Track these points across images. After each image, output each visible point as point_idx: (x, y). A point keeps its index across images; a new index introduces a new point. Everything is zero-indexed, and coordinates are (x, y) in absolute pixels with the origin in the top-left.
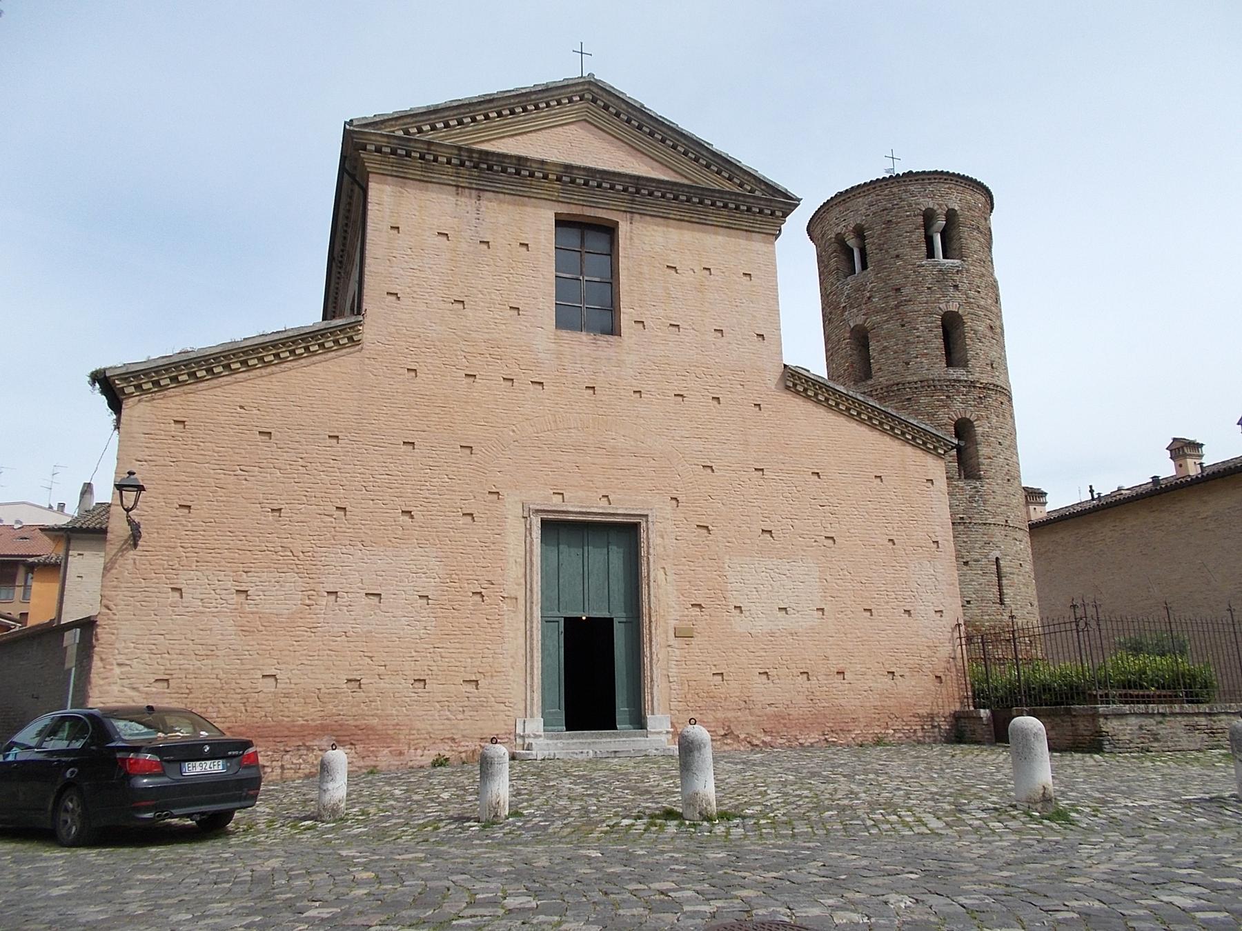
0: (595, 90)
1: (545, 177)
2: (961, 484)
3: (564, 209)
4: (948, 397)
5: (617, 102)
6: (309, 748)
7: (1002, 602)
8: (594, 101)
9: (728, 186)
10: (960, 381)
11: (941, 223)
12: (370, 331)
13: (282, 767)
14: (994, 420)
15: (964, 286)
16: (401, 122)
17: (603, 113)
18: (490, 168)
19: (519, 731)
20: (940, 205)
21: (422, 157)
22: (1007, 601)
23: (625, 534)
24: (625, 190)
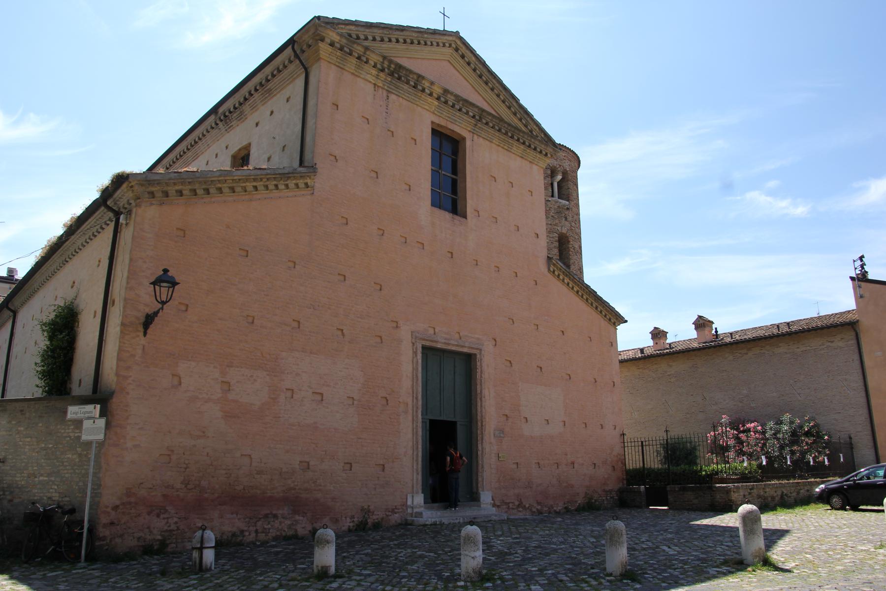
0: (459, 42)
1: (431, 95)
3: (437, 120)
5: (471, 55)
6: (275, 516)
8: (457, 50)
9: (524, 129)
11: (559, 177)
12: (319, 182)
13: (256, 531)
15: (570, 219)
16: (348, 27)
17: (460, 59)
18: (399, 78)
19: (409, 503)
21: (359, 58)
23: (468, 362)
24: (474, 117)
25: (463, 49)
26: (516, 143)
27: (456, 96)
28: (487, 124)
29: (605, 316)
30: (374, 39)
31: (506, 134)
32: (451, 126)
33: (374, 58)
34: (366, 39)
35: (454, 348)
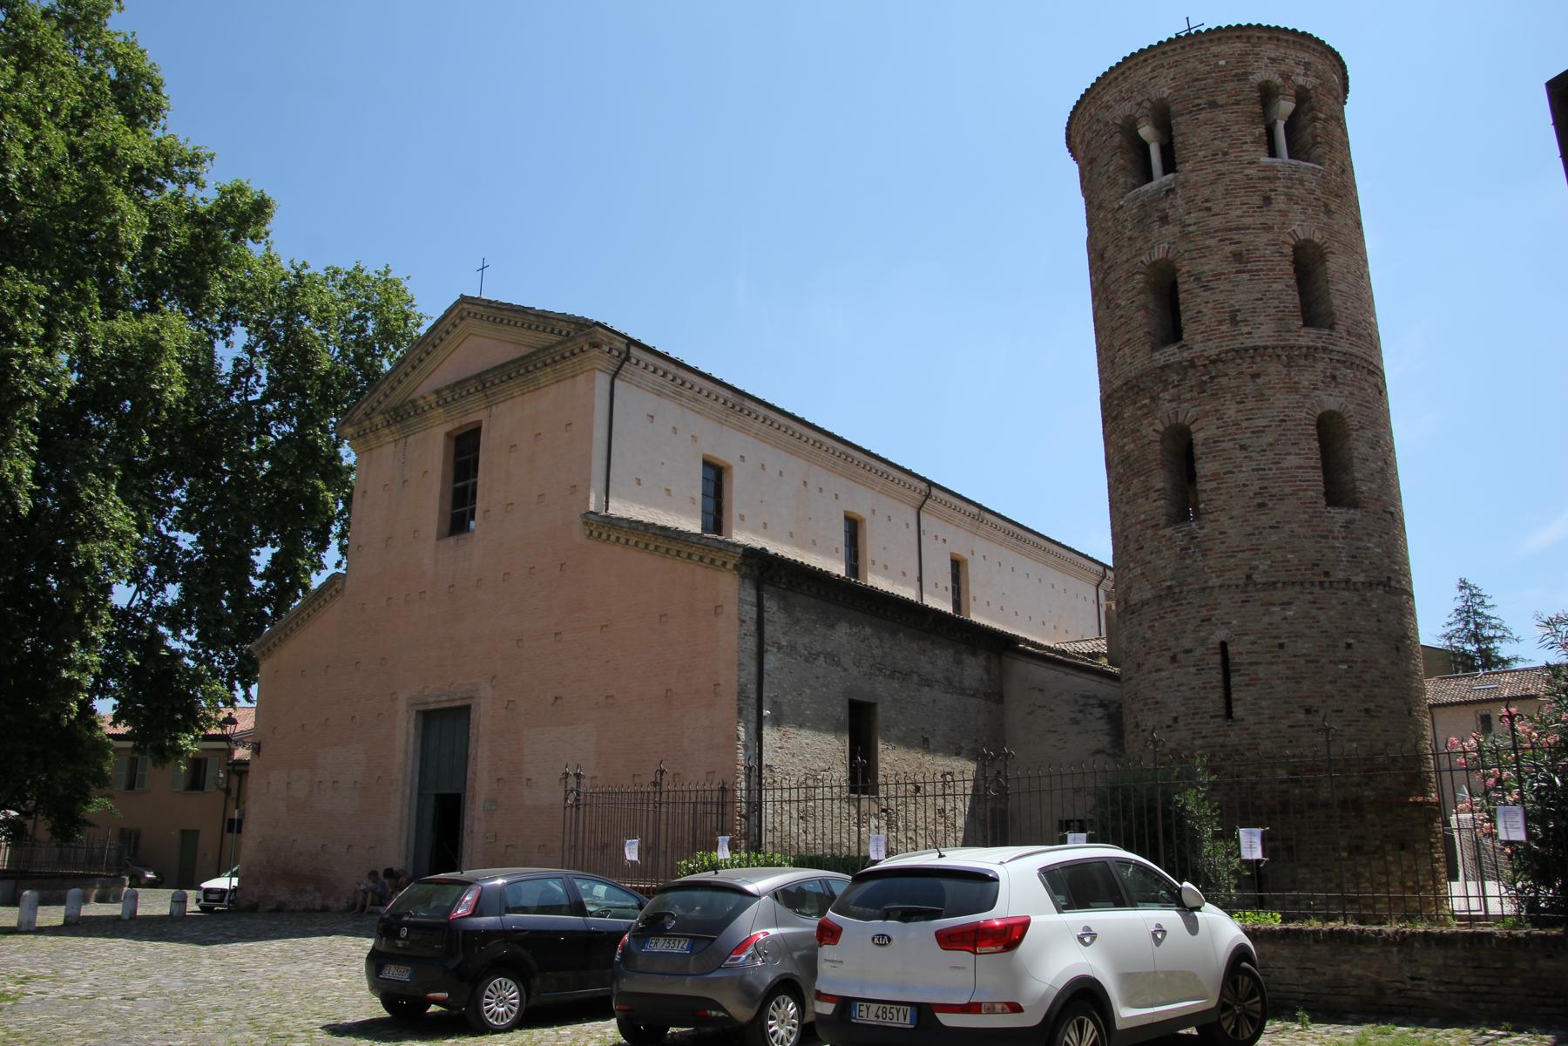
2: (1168, 532)
3: (449, 427)
4: (1153, 399)
14: (1231, 411)
20: (1139, 104)
22: (1238, 711)
25: (474, 309)
26: (538, 373)
27: (448, 387)
28: (493, 384)
29: (701, 559)
30: (386, 396)
31: (519, 374)
32: (465, 421)
33: (378, 419)
34: (380, 403)
35: (446, 705)
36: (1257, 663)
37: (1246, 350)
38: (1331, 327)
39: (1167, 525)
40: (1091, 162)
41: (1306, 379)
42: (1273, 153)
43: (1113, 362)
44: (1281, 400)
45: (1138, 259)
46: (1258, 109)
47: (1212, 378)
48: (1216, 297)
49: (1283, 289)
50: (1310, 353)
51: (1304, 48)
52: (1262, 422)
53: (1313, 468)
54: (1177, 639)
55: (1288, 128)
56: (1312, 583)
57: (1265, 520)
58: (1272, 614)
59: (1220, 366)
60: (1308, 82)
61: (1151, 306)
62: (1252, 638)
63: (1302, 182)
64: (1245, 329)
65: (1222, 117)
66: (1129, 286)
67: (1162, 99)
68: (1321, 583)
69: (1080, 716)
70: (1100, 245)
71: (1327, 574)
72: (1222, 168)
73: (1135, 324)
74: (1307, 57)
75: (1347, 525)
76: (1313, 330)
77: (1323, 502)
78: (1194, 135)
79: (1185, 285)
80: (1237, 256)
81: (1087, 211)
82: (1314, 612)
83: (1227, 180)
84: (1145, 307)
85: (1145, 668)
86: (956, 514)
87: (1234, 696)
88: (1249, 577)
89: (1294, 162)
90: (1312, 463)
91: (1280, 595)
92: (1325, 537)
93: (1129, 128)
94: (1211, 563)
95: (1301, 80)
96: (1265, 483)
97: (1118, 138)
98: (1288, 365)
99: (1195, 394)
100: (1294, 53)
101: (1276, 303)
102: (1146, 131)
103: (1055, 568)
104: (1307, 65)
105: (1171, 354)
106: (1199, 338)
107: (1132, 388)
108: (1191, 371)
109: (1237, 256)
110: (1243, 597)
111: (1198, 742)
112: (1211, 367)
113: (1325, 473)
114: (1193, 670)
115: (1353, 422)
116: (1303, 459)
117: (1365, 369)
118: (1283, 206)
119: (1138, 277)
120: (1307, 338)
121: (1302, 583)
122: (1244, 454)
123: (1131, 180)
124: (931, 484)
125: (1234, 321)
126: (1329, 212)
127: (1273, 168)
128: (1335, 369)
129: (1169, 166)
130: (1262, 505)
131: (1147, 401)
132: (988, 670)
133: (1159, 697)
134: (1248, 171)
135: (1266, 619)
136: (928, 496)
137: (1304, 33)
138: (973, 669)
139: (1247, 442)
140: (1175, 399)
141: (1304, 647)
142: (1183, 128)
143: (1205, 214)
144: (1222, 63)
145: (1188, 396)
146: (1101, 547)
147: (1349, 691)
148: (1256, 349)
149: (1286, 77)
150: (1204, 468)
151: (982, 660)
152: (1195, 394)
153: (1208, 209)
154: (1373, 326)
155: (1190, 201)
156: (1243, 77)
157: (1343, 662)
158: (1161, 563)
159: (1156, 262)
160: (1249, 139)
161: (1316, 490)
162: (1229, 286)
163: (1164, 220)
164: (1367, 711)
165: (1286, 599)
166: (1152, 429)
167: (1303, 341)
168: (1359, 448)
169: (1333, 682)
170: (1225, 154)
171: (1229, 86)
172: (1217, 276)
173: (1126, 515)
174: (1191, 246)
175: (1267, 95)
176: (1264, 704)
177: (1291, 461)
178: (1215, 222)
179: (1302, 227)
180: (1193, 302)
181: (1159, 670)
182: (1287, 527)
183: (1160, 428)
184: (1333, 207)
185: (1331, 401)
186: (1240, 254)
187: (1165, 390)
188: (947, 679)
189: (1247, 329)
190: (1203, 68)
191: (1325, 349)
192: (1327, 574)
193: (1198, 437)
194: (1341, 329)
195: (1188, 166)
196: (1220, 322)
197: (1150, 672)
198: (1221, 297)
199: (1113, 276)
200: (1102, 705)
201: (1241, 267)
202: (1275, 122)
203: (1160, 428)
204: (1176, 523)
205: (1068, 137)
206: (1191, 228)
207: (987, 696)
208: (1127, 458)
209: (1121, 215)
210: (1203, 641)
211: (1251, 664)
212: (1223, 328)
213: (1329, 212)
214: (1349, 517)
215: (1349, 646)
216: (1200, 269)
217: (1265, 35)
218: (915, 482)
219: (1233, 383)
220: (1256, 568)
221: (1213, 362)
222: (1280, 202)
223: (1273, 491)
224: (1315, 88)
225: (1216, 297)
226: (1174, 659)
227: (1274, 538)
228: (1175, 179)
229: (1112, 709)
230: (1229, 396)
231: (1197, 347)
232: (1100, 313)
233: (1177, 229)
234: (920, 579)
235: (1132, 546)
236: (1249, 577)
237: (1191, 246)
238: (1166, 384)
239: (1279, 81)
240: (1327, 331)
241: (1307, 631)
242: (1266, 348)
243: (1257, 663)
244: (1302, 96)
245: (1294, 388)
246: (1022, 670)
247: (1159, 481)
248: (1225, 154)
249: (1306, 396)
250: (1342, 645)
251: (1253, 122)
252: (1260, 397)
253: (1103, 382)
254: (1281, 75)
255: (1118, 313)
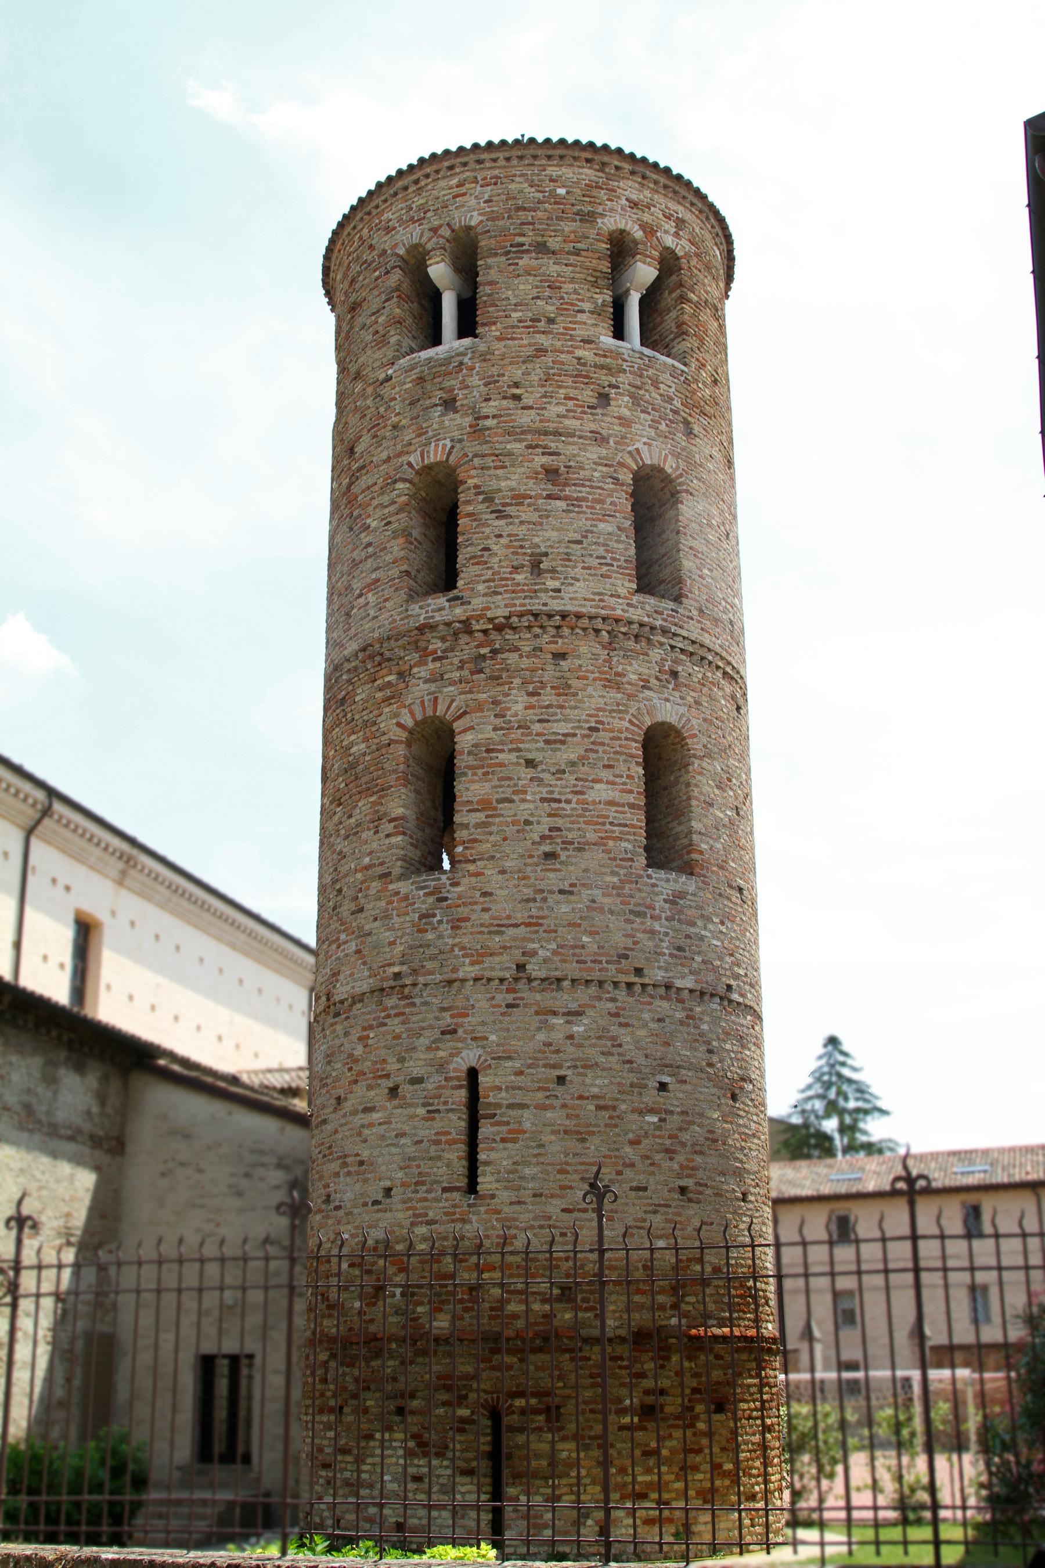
2: (404, 887)
4: (401, 674)
7: (472, 1187)
10: (432, 627)
14: (518, 704)
20: (435, 230)
22: (486, 1182)
36: (523, 1106)
37: (550, 616)
38: (678, 599)
39: (402, 877)
40: (354, 308)
41: (633, 671)
42: (619, 332)
43: (348, 614)
44: (595, 697)
45: (404, 459)
46: (605, 266)
47: (495, 652)
48: (512, 529)
49: (614, 531)
50: (643, 633)
51: (681, 200)
52: (562, 728)
53: (632, 806)
54: (401, 1060)
55: (647, 304)
56: (616, 984)
57: (553, 880)
58: (552, 1028)
59: (509, 635)
60: (681, 246)
61: (416, 533)
62: (517, 1064)
63: (656, 384)
64: (551, 584)
65: (552, 268)
66: (386, 499)
67: (469, 228)
68: (629, 985)
69: (245, 1183)
70: (350, 434)
71: (639, 972)
72: (544, 340)
73: (388, 558)
74: (682, 212)
75: (675, 899)
76: (652, 600)
77: (644, 861)
78: (508, 287)
79: (469, 506)
80: (551, 473)
81: (339, 382)
82: (615, 1031)
83: (548, 360)
84: (406, 533)
85: (348, 1106)
86: (91, 848)
87: (482, 1157)
88: (521, 967)
89: (647, 351)
90: (631, 798)
91: (565, 999)
92: (638, 914)
93: (415, 265)
94: (465, 940)
95: (669, 241)
96: (559, 822)
97: (396, 276)
98: (609, 646)
99: (466, 673)
100: (663, 202)
101: (601, 551)
102: (439, 271)
103: (247, 954)
104: (680, 223)
105: (438, 608)
106: (481, 588)
107: (371, 657)
108: (464, 638)
109: (551, 473)
110: (510, 998)
111: (422, 1230)
112: (494, 635)
113: (650, 820)
114: (421, 1111)
115: (696, 745)
116: (616, 791)
117: (715, 667)
118: (625, 412)
119: (400, 485)
120: (644, 609)
121: (601, 983)
122: (530, 773)
123: (407, 342)
124: (52, 793)
125: (535, 565)
126: (689, 433)
127: (618, 355)
128: (676, 661)
129: (467, 327)
130: (550, 856)
131: (391, 678)
132: (102, 1099)
133: (365, 1154)
134: (580, 353)
135: (541, 1037)
136: (46, 812)
137: (679, 177)
138: (76, 1094)
139: (537, 756)
140: (436, 678)
141: (596, 1084)
142: (494, 274)
143: (511, 404)
144: (562, 191)
145: (456, 675)
146: (297, 909)
147: (658, 1157)
148: (564, 616)
149: (650, 231)
150: (470, 789)
151: (92, 1080)
152: (466, 673)
153: (517, 398)
154: (737, 610)
155: (490, 382)
156: (588, 218)
157: (652, 1111)
158: (389, 936)
159: (428, 468)
160: (587, 306)
161: (632, 842)
162: (534, 517)
163: (449, 404)
164: (683, 1190)
165: (573, 1006)
166: (396, 722)
167: (635, 614)
168: (702, 781)
169: (635, 1143)
170: (551, 321)
171: (568, 227)
172: (519, 499)
173: (342, 856)
174: (485, 449)
175: (621, 250)
176: (527, 1171)
177: (601, 792)
178: (525, 419)
179: (653, 450)
180: (476, 531)
181: (367, 1110)
182: (586, 893)
183: (409, 722)
184: (696, 429)
185: (668, 710)
186: (556, 471)
187: (421, 663)
188: (29, 1109)
189: (556, 584)
190: (532, 193)
191: (665, 631)
192: (639, 972)
193: (464, 741)
194: (690, 604)
195: (495, 331)
196: (516, 569)
197: (355, 1112)
198: (522, 531)
199: (365, 481)
200: (281, 1166)
201: (555, 490)
202: (627, 292)
203: (409, 722)
204: (418, 872)
205: (326, 271)
206: (489, 423)
207: (95, 1142)
208: (353, 766)
209: (386, 391)
210: (441, 1066)
211: (511, 1106)
212: (519, 578)
213: (689, 433)
214: (677, 887)
215: (663, 1087)
216: (494, 484)
217: (627, 167)
218: (27, 787)
219: (525, 663)
220: (534, 953)
221: (499, 628)
222: (621, 405)
223: (570, 836)
224: (687, 256)
225: (512, 529)
226: (393, 1091)
227: (565, 908)
228: (473, 349)
229: (298, 1171)
230: (517, 681)
231: (478, 603)
232: (338, 539)
233: (468, 420)
234: (18, 945)
235: (347, 907)
236: (521, 967)
237: (485, 449)
238: (425, 653)
239: (639, 234)
240: (671, 605)
241: (602, 1059)
242: (579, 616)
243: (523, 1106)
244: (669, 265)
245: (614, 682)
246: (163, 1100)
247: (400, 803)
248: (551, 321)
249: (630, 696)
250: (653, 1084)
251: (594, 284)
252: (563, 689)
253: (332, 644)
254: (643, 226)
255: (365, 538)
